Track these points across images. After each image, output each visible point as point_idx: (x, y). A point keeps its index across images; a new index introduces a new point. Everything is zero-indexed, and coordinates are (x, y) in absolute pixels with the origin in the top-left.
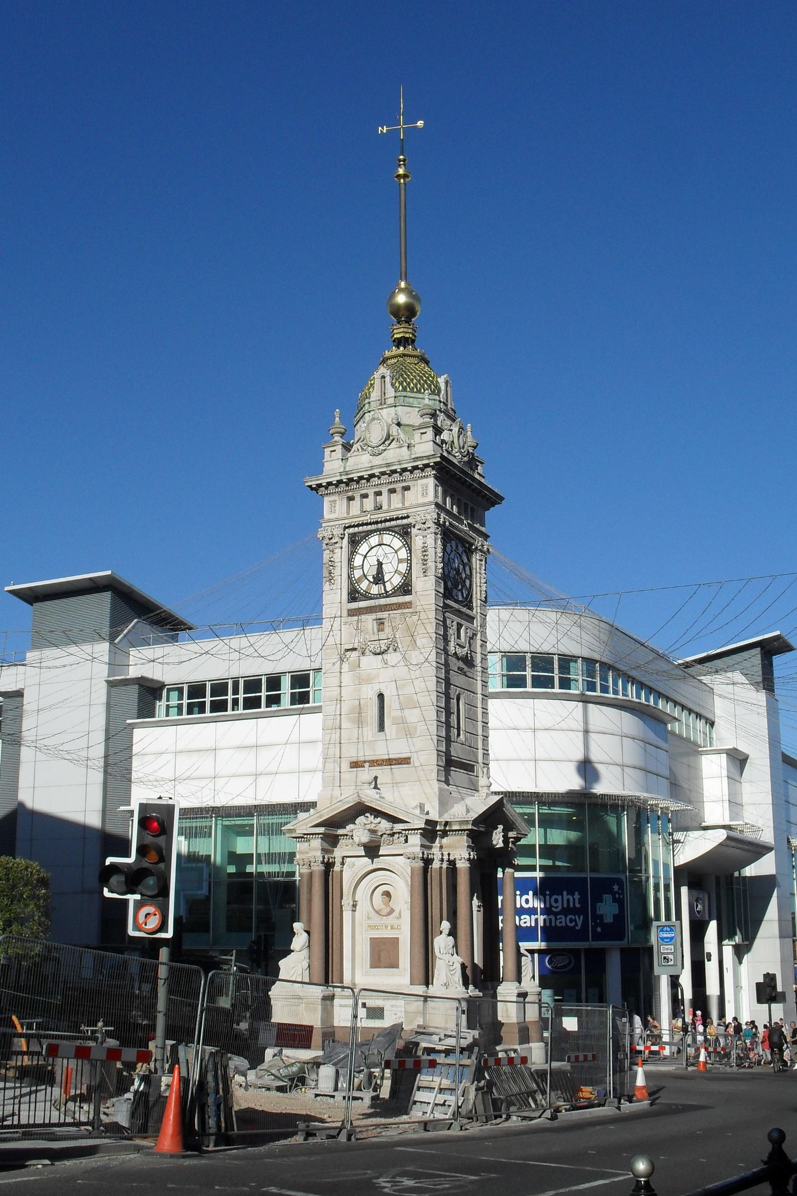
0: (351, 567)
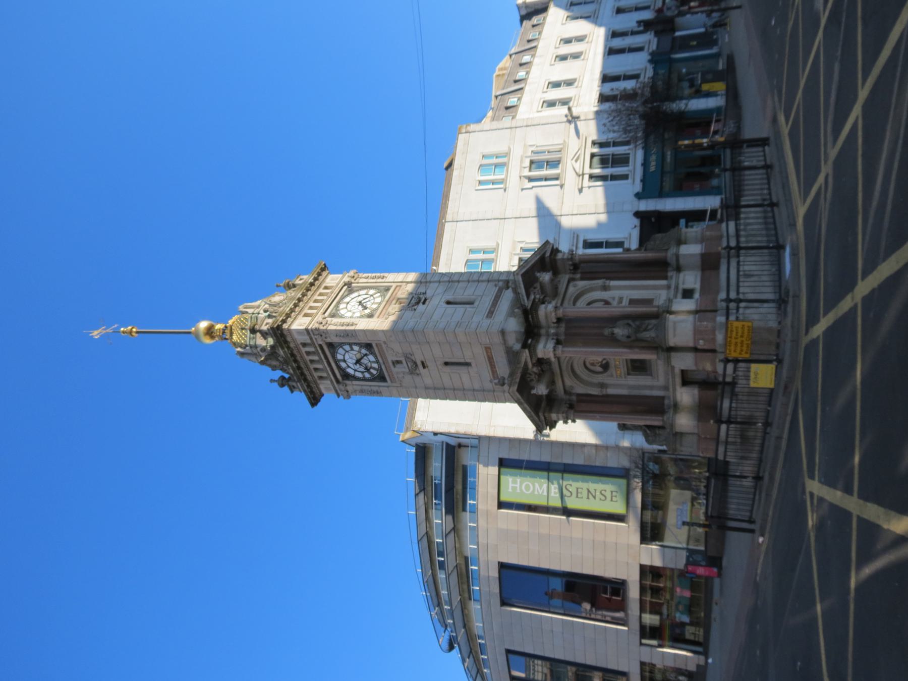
0: (364, 379)
